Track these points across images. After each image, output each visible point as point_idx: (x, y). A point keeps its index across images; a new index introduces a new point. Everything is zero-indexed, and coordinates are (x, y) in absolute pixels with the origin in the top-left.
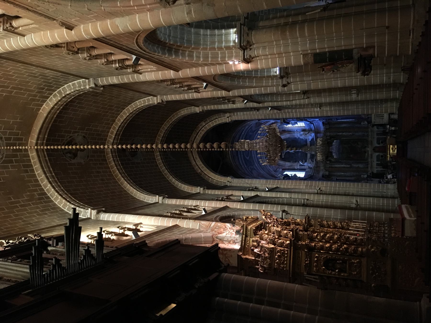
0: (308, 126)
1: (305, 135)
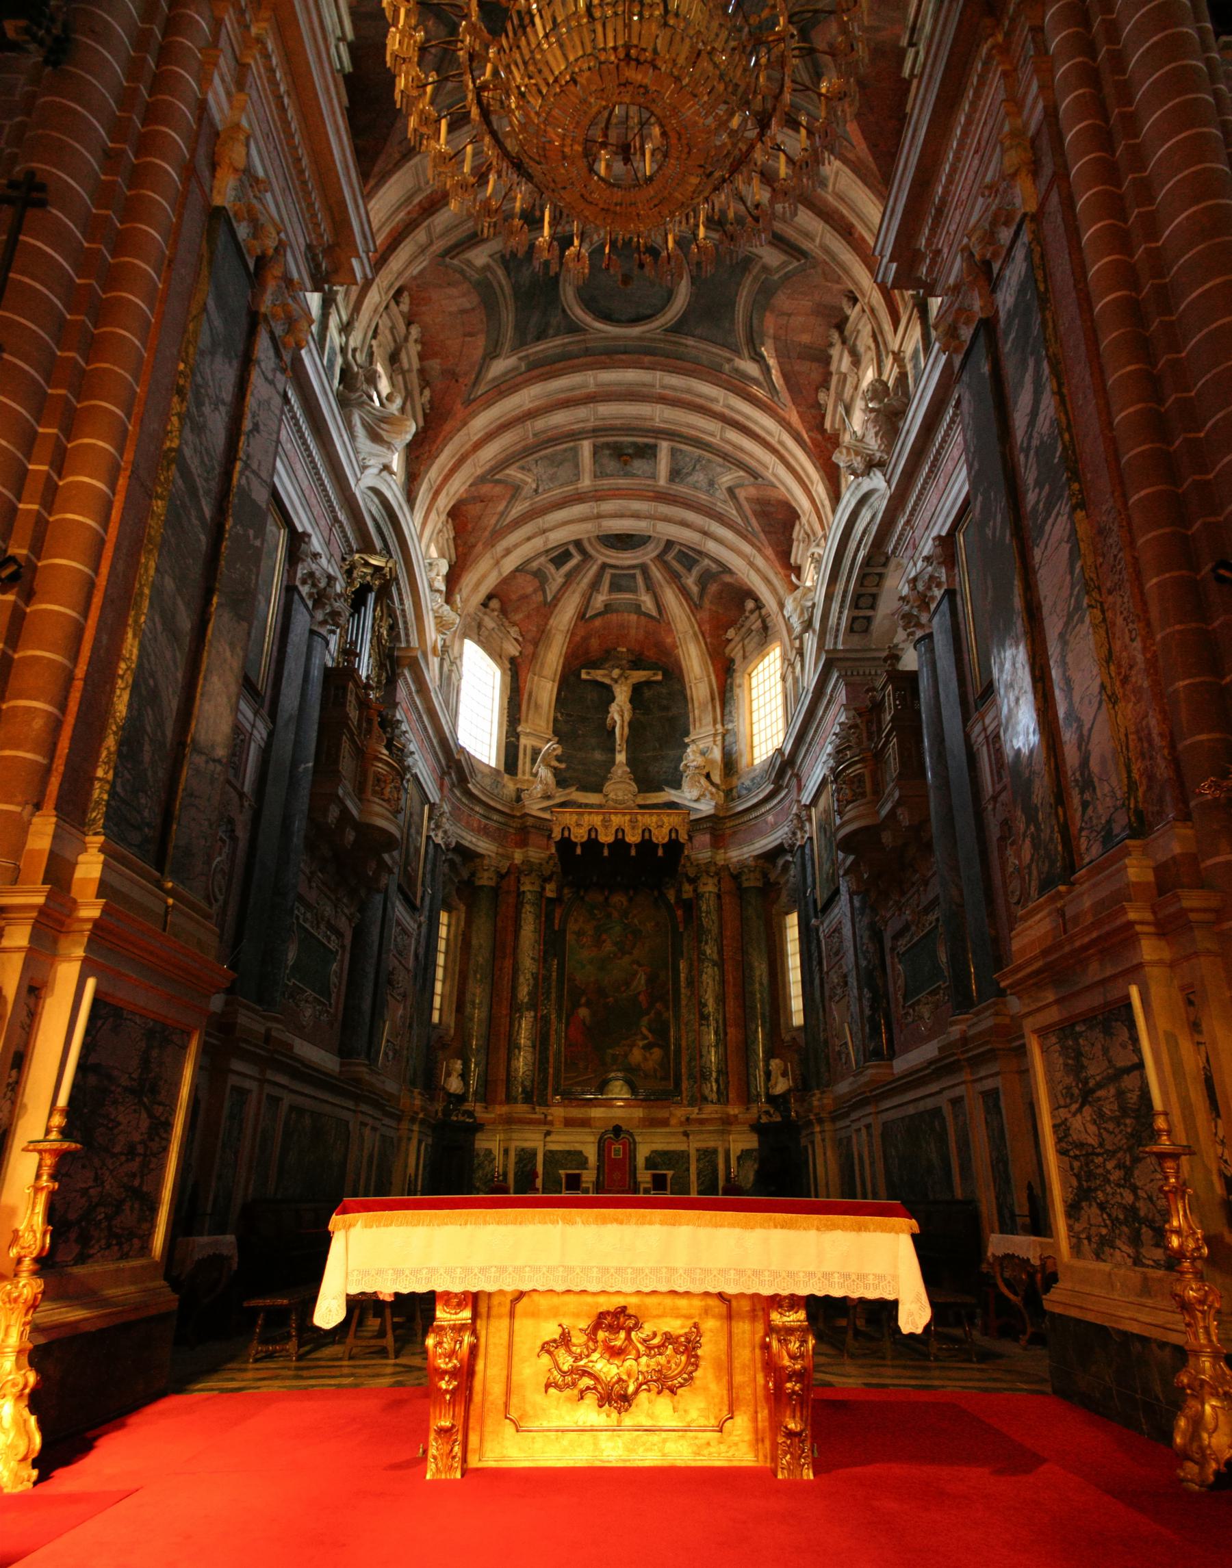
0: (753, 780)
1: (704, 772)
